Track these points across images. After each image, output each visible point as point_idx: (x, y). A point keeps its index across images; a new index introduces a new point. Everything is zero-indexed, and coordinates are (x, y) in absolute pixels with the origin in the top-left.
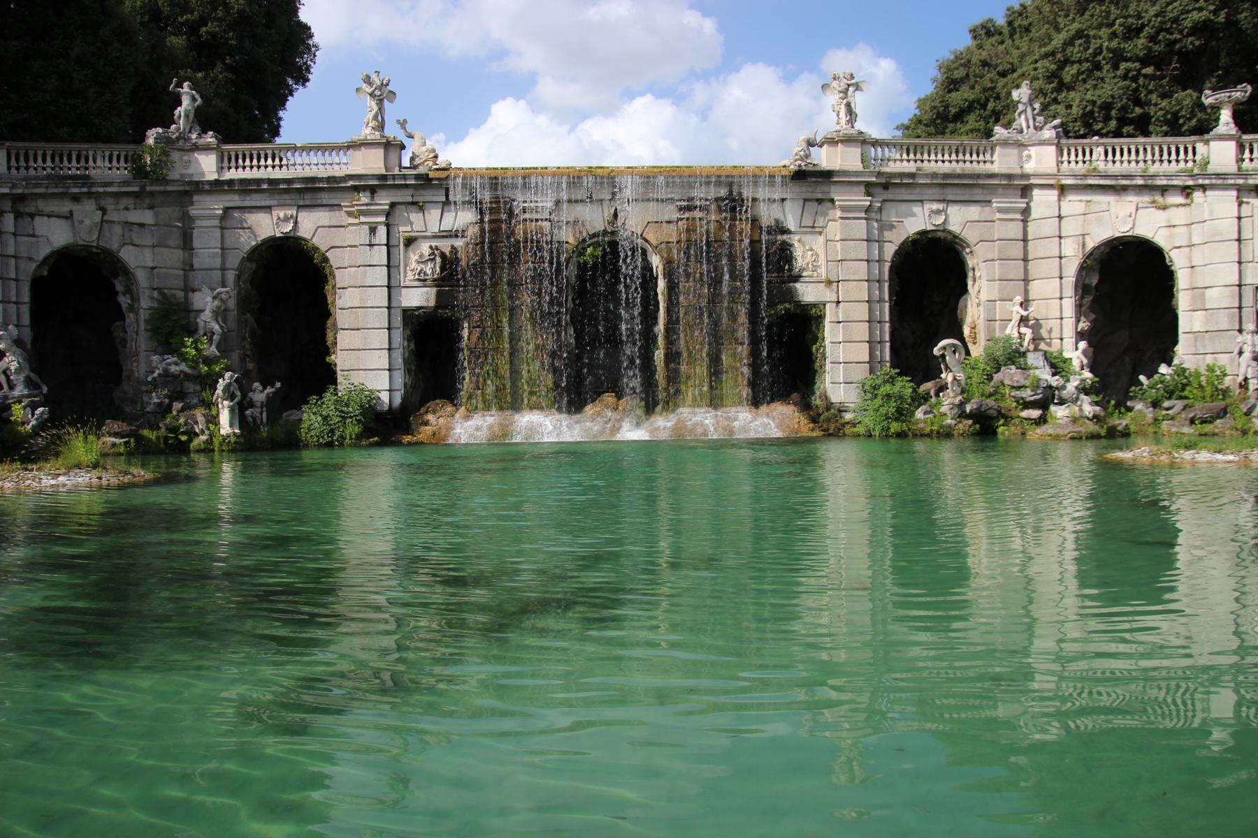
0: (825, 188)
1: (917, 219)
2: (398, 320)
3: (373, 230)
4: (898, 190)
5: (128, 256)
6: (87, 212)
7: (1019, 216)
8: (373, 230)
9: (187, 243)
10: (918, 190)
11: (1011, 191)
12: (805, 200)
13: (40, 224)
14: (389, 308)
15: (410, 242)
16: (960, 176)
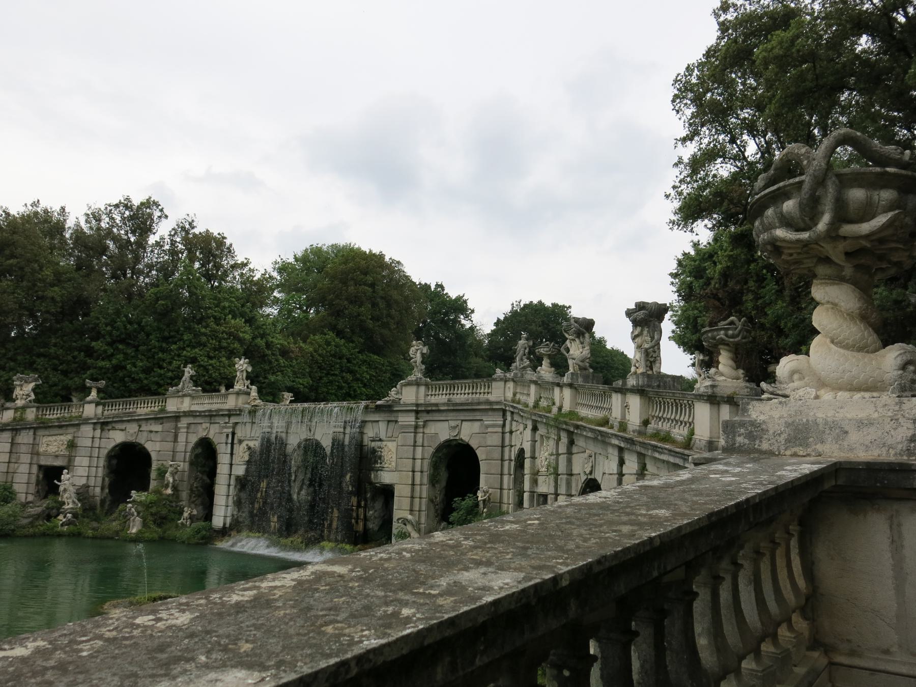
0: (396, 414)
1: (442, 431)
2: (233, 482)
3: (227, 436)
4: (435, 414)
5: (149, 446)
6: (133, 428)
7: (500, 430)
8: (227, 436)
9: (175, 440)
10: (444, 414)
11: (496, 413)
12: (389, 421)
13: (112, 434)
14: (230, 475)
15: (240, 442)
16: (462, 404)
